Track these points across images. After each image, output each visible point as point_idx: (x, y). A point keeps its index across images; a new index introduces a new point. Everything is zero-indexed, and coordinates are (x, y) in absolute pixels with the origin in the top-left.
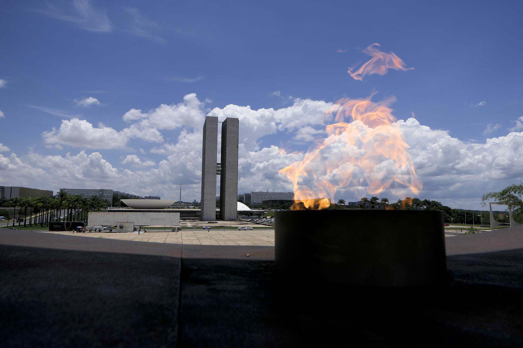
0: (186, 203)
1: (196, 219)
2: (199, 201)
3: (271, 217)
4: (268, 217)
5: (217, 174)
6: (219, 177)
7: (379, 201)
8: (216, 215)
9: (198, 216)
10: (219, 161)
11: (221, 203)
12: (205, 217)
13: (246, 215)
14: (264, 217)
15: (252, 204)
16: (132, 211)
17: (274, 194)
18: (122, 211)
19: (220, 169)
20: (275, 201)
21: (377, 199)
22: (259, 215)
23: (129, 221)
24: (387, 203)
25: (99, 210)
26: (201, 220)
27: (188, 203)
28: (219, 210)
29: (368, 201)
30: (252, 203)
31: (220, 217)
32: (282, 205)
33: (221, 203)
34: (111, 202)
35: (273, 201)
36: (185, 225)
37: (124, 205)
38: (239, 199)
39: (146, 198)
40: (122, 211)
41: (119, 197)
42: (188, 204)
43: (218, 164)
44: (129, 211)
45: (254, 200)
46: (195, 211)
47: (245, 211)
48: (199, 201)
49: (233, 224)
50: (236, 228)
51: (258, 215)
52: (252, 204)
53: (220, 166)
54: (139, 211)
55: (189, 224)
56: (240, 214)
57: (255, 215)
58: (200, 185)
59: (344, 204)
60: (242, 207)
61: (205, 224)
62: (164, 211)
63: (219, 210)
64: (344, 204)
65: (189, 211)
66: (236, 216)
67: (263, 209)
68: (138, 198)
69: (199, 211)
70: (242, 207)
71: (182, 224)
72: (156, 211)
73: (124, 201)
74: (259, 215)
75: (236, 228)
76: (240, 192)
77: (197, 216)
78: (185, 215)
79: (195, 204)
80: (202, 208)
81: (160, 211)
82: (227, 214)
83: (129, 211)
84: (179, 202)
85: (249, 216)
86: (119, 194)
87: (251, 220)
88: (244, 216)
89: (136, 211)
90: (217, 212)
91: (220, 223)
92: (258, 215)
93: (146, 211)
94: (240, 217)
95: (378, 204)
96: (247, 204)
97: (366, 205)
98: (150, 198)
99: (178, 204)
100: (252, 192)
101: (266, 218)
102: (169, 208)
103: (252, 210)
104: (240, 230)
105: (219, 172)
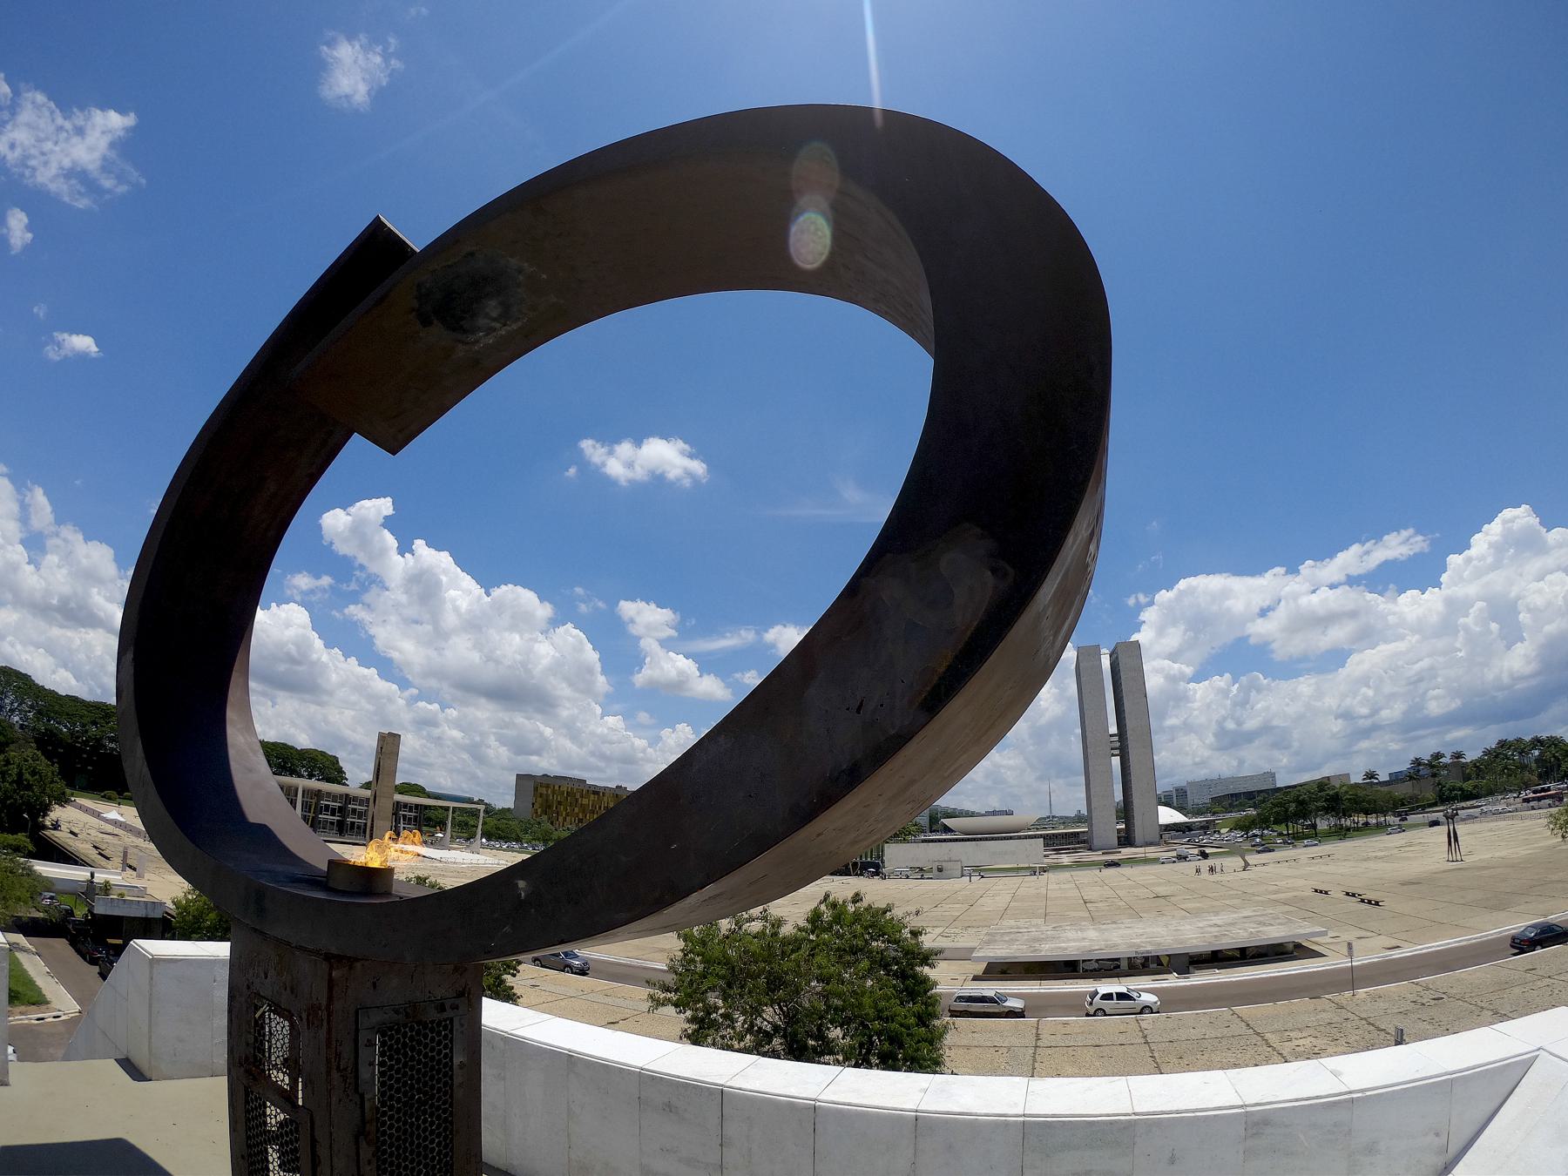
0: (1061, 818)
1: (1080, 848)
2: (1084, 812)
3: (1231, 830)
4: (1223, 831)
5: (1113, 755)
6: (1116, 761)
7: (1446, 760)
8: (1119, 838)
9: (1084, 842)
10: (1113, 729)
11: (1125, 812)
12: (1096, 842)
13: (1177, 832)
14: (1215, 832)
15: (1190, 807)
16: (963, 840)
17: (1233, 780)
18: (945, 840)
19: (1118, 744)
20: (1236, 794)
21: (1443, 756)
22: (1205, 828)
23: (953, 859)
24: (1463, 760)
25: (904, 839)
26: (1090, 849)
27: (1066, 817)
28: (1124, 826)
29: (1424, 764)
30: (1190, 803)
31: (1126, 840)
32: (1251, 802)
33: (1125, 812)
34: (928, 826)
35: (1232, 795)
36: (1059, 861)
37: (947, 830)
38: (1163, 800)
39: (988, 814)
40: (945, 840)
41: (939, 815)
42: (1065, 821)
43: (1111, 736)
44: (956, 840)
45: (1194, 799)
46: (1078, 833)
47: (1175, 824)
48: (1084, 812)
49: (1151, 852)
50: (1155, 861)
51: (1202, 828)
52: (1190, 807)
53: (1116, 738)
54: (974, 840)
55: (1066, 859)
56: (1165, 830)
57: (1198, 829)
58: (1082, 779)
59: (1377, 779)
60: (1168, 816)
61: (1097, 856)
62: (1019, 838)
63: (1124, 826)
64: (1377, 779)
65: (1066, 834)
66: (1158, 836)
67: (1214, 814)
68: (973, 814)
69: (1084, 832)
70: (1168, 816)
71: (1053, 858)
72: (1005, 838)
73: (946, 821)
74: (1205, 828)
75: (1155, 861)
76: (1164, 785)
77: (1082, 843)
78: (1056, 842)
79: (1079, 819)
80: (1091, 826)
81: (1011, 838)
82: (1138, 834)
83: (956, 840)
84: (1049, 817)
85: (1184, 833)
86: (939, 810)
87: (1189, 841)
88: (1173, 833)
89: (968, 840)
90: (1119, 831)
91: (1127, 852)
92: (1202, 828)
93: (986, 839)
94: (1166, 836)
95: (1446, 766)
96: (1180, 809)
97: (1421, 773)
98: (994, 813)
99: (1041, 823)
100: (1188, 783)
101: (1219, 831)
102: (1029, 829)
103: (1191, 820)
104: (1163, 863)
105: (1117, 752)
